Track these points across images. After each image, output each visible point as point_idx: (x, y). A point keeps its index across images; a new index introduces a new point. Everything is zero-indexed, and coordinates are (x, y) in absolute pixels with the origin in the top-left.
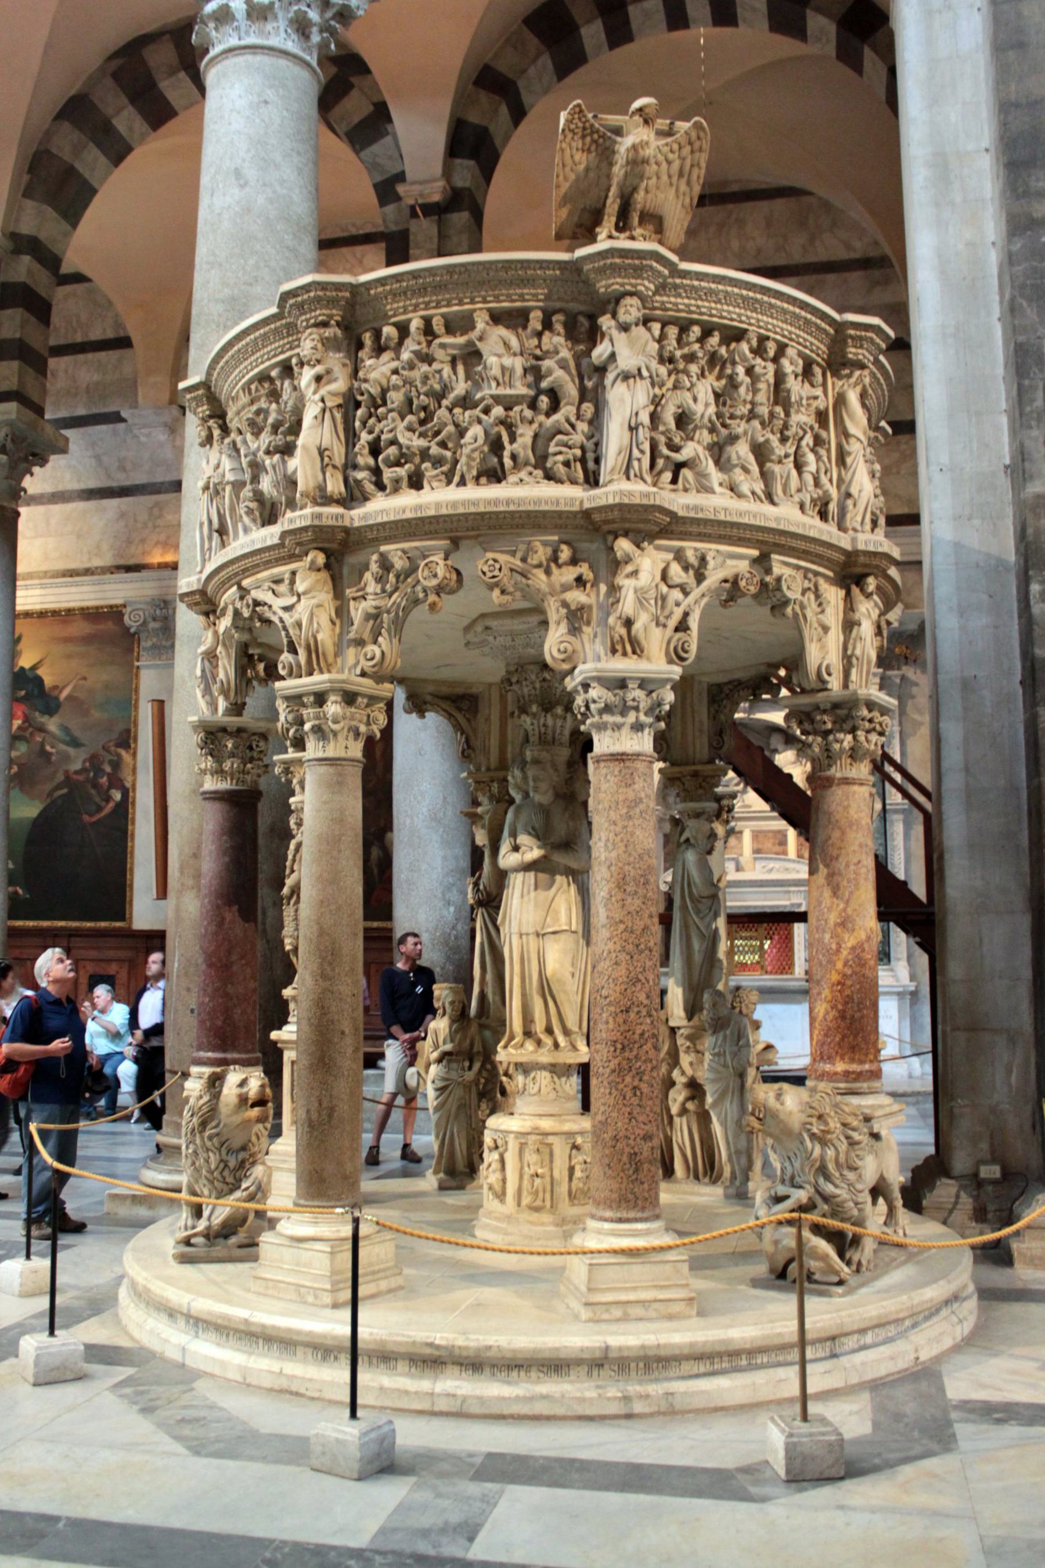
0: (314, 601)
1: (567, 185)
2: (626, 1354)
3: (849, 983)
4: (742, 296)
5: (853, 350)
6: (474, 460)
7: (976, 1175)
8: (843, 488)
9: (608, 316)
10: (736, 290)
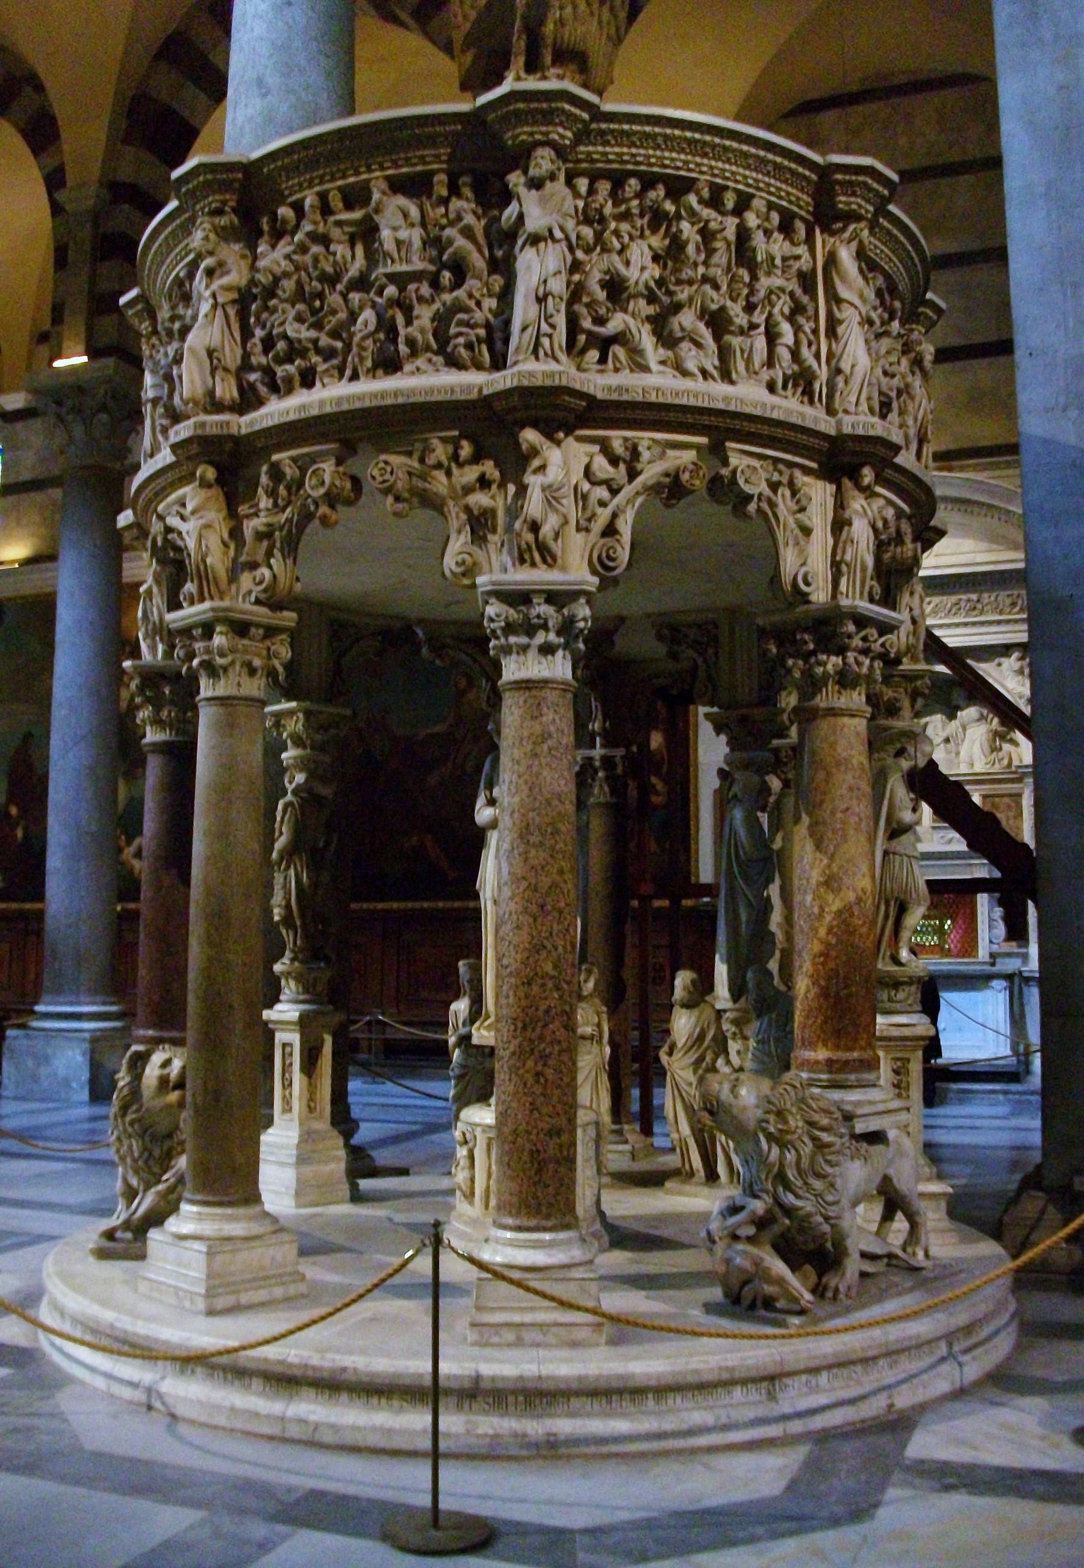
0: (202, 522)
1: (468, 25)
2: (500, 1385)
3: (833, 953)
4: (686, 139)
5: (843, 198)
7: (1069, 1186)
8: (834, 363)
9: (518, 172)
10: (677, 132)
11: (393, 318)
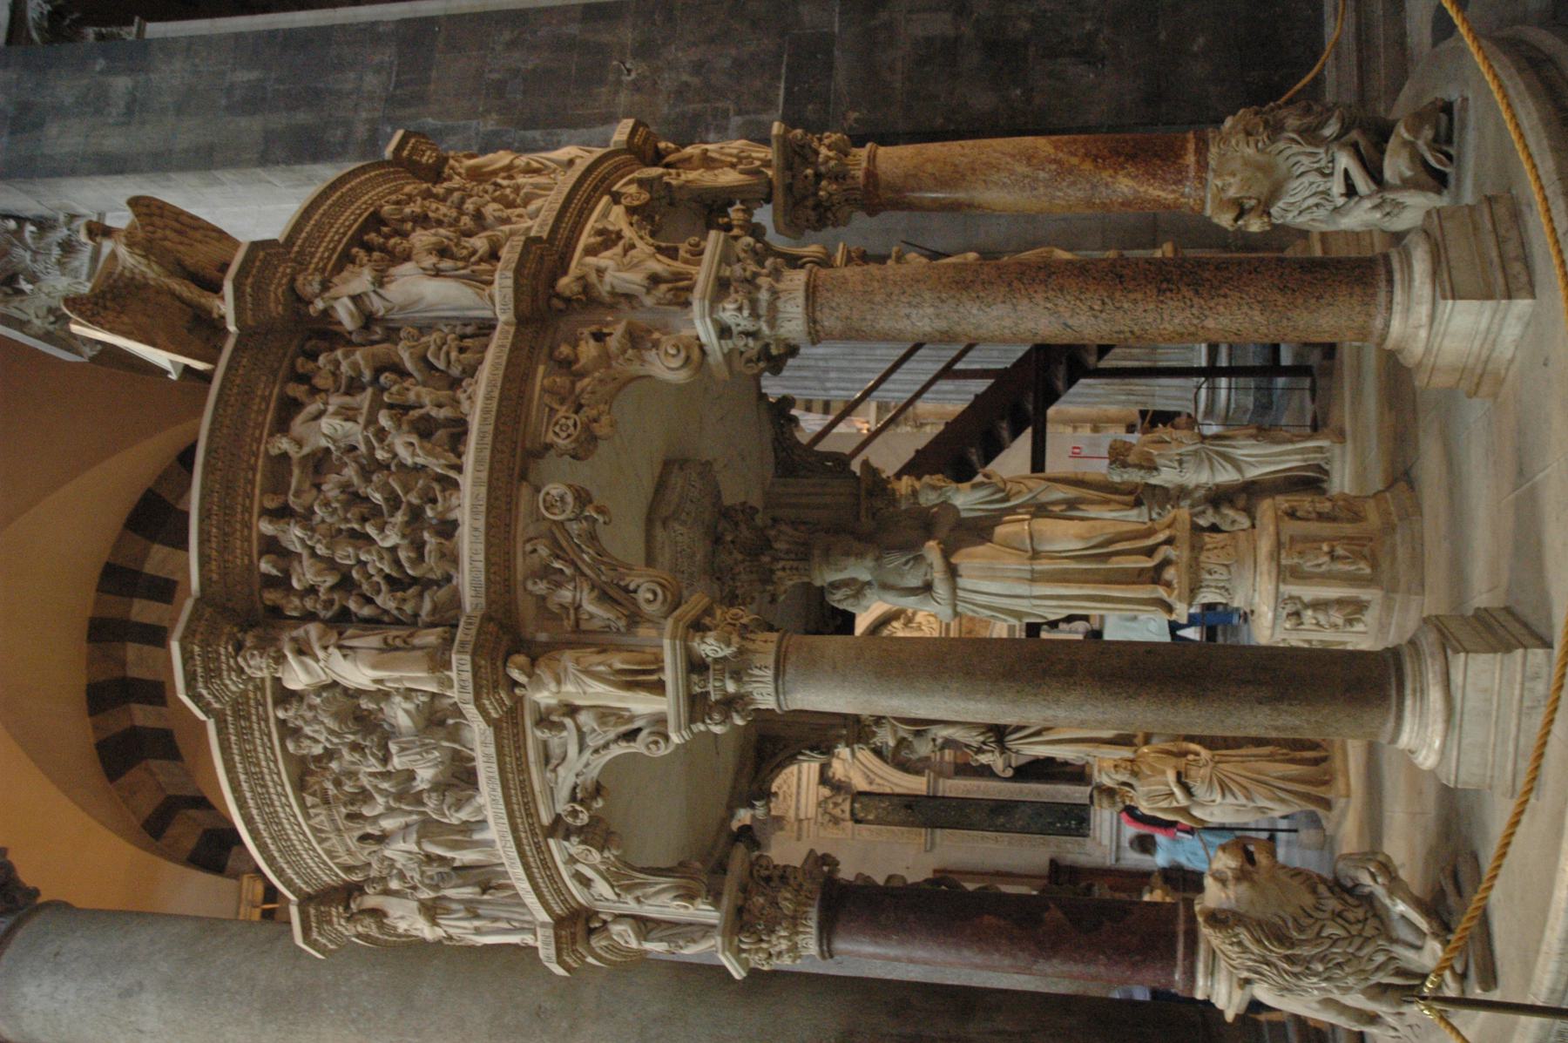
5: (425, 158)
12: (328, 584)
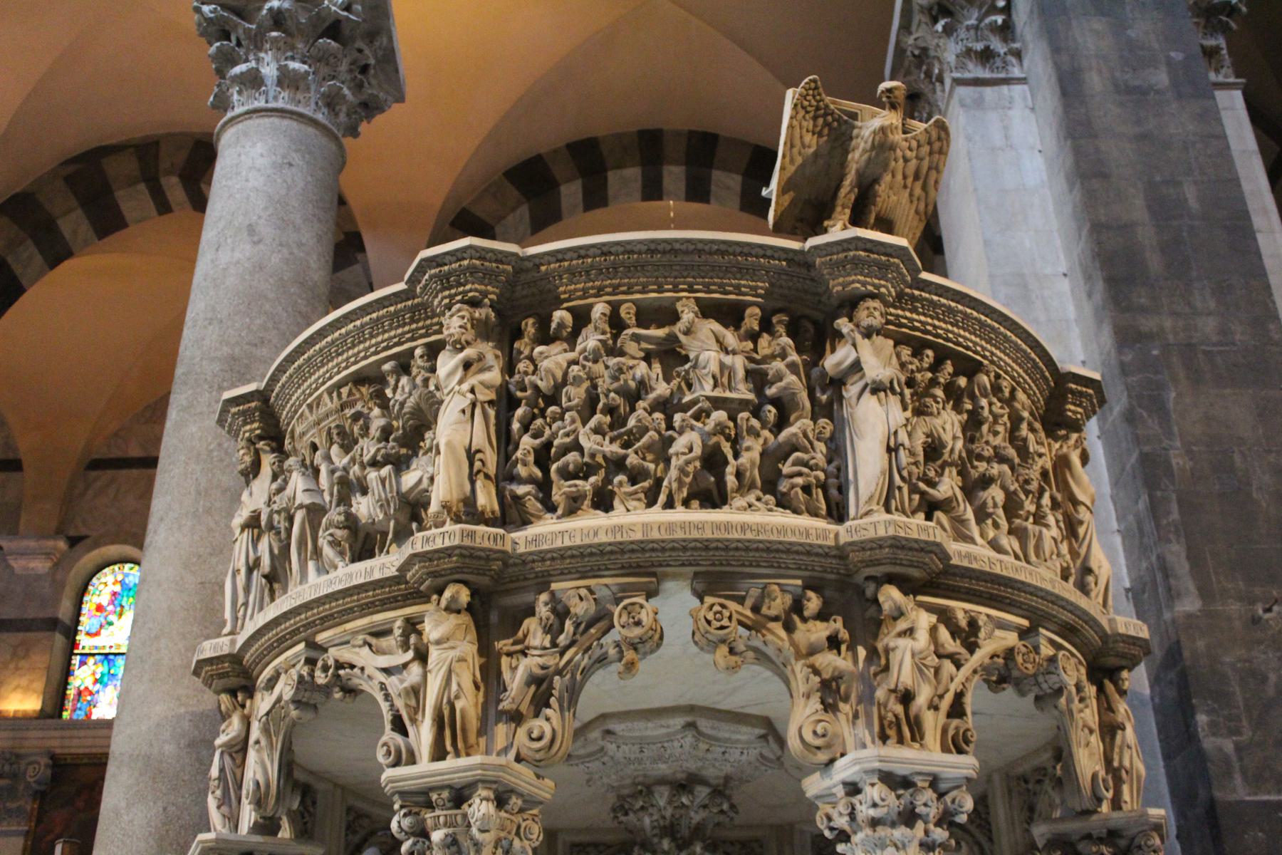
0: (451, 654)
4: (979, 321)
5: (1072, 407)
6: (687, 475)
11: (717, 446)
12: (539, 383)
